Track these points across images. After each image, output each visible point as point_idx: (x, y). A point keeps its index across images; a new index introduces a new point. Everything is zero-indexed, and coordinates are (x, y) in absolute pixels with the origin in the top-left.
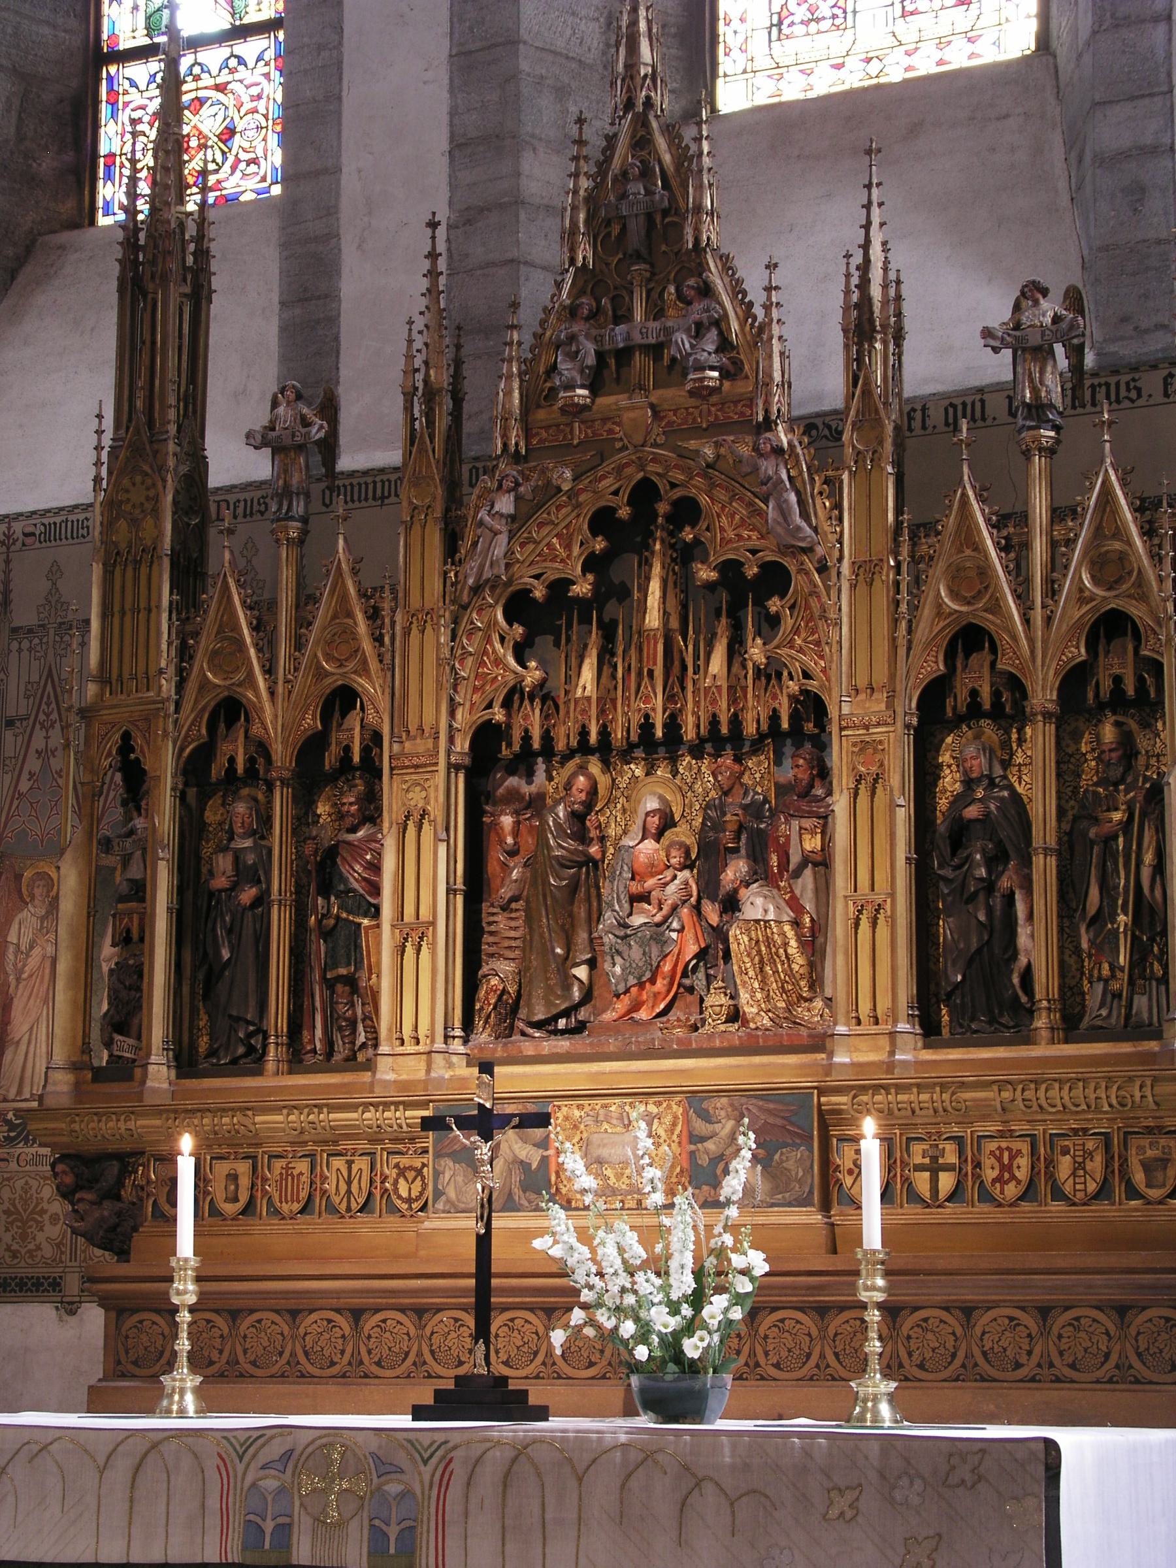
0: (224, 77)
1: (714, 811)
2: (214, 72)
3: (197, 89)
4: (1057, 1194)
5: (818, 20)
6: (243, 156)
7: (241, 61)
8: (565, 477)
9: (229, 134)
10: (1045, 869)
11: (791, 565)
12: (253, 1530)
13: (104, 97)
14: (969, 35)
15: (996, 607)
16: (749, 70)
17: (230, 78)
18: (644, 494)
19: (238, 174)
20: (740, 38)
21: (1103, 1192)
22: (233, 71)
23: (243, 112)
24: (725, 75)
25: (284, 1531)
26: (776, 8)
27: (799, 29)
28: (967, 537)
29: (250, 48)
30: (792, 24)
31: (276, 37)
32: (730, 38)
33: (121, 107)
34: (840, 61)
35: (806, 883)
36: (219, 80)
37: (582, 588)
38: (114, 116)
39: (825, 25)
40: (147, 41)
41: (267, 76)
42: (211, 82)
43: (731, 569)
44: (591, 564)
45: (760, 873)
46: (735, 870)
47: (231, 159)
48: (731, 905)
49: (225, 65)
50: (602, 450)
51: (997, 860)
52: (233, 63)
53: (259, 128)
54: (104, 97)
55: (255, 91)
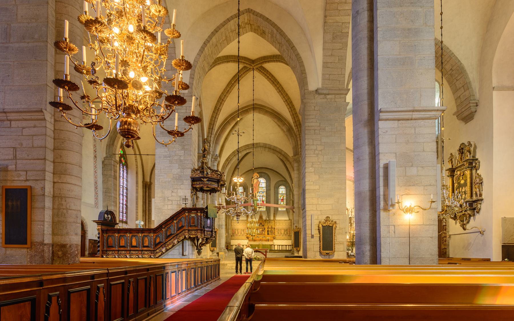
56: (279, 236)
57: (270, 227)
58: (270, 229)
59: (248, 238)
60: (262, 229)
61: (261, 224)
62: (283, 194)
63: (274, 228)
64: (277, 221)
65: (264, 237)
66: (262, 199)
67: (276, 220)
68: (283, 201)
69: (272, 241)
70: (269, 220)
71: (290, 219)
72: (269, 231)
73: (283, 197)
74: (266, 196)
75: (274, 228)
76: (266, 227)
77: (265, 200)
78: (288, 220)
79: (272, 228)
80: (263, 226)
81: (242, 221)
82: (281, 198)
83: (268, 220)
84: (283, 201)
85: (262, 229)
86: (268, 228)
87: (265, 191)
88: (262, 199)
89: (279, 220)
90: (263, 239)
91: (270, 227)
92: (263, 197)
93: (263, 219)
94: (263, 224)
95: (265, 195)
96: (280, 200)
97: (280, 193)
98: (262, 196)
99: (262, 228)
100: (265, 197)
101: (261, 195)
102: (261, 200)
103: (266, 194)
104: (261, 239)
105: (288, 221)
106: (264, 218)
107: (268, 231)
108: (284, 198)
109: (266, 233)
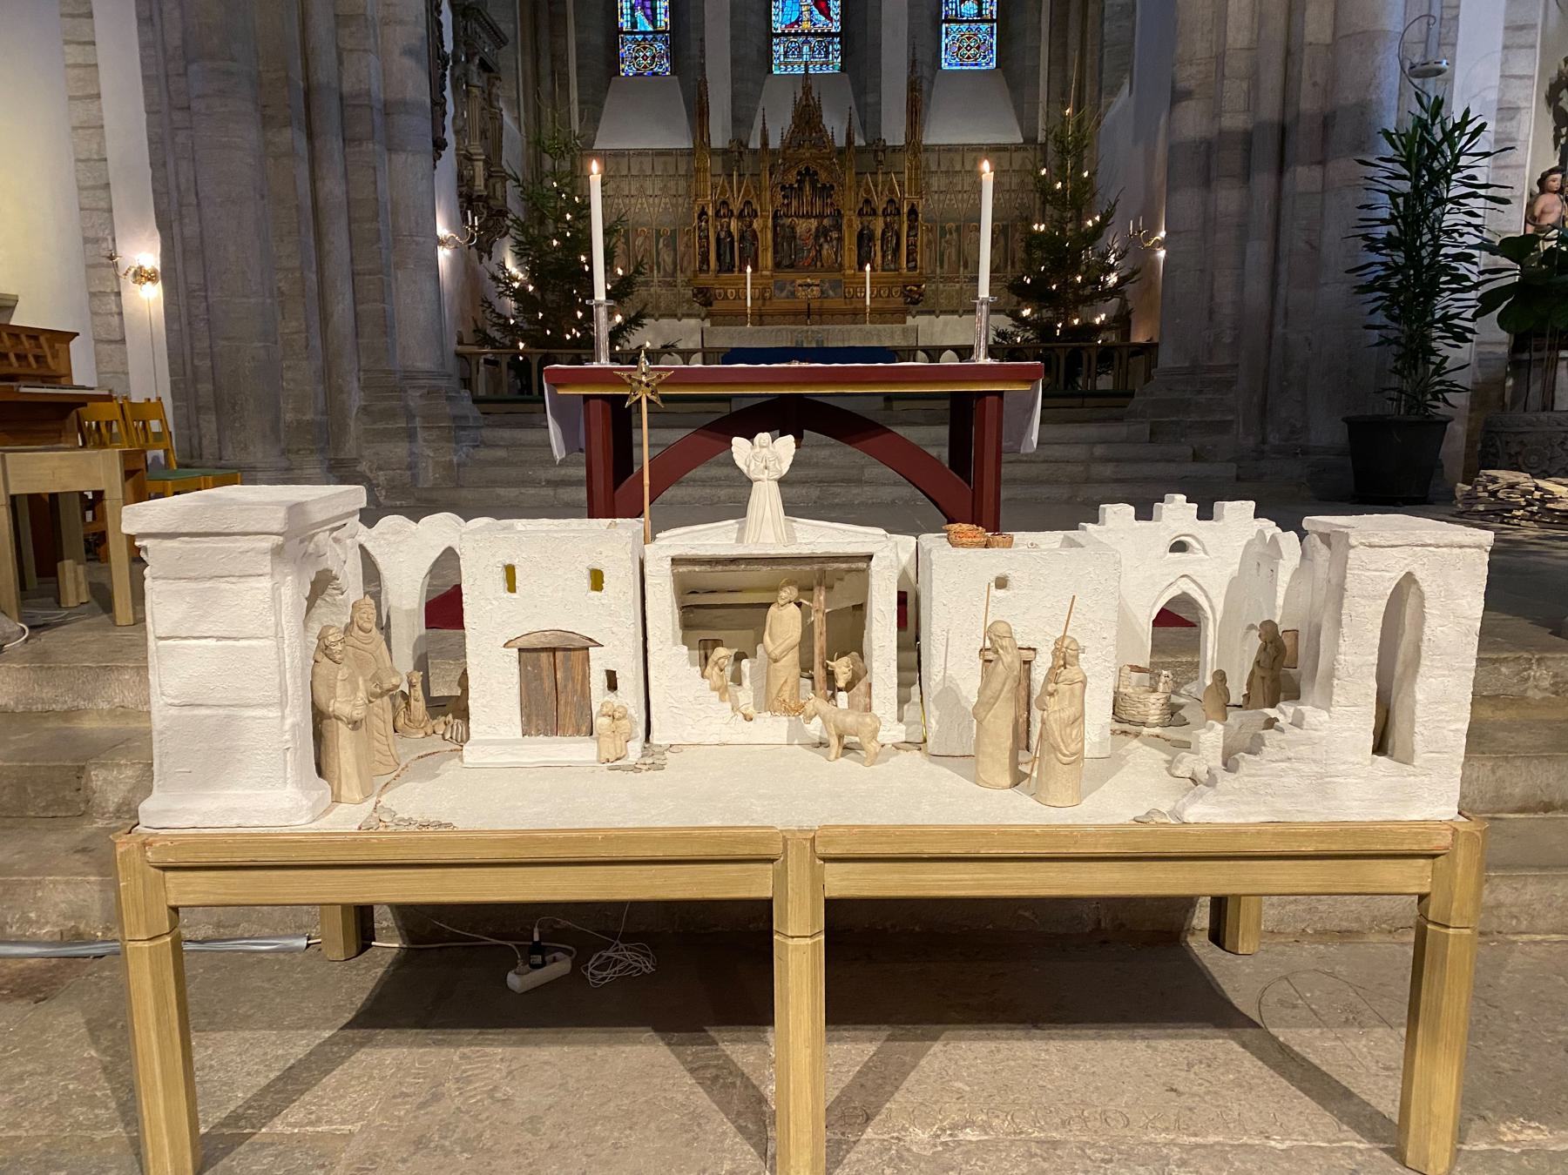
1: (817, 229)
4: (881, 296)
8: (793, 164)
9: (654, 57)
10: (879, 243)
11: (835, 185)
12: (797, 342)
15: (872, 196)
18: (807, 169)
21: (888, 296)
25: (802, 342)
28: (867, 184)
35: (835, 243)
37: (796, 186)
43: (824, 185)
44: (797, 181)
45: (826, 241)
46: (822, 240)
48: (821, 246)
50: (801, 160)
51: (870, 240)
56: (946, 280)
57: (880, 204)
58: (879, 225)
59: (705, 297)
60: (814, 223)
61: (808, 174)
63: (913, 212)
64: (933, 158)
65: (836, 285)
67: (927, 149)
69: (899, 315)
70: (877, 150)
71: (1030, 140)
72: (871, 238)
75: (913, 212)
76: (849, 202)
78: (1017, 148)
79: (893, 208)
80: (826, 191)
81: (659, 161)
83: (860, 150)
85: (814, 223)
86: (866, 209)
89: (950, 149)
90: (828, 304)
91: (880, 204)
93: (821, 130)
94: (823, 176)
99: (817, 211)
104: (815, 305)
105: (1018, 157)
106: (835, 126)
107: (860, 235)
109: (850, 256)
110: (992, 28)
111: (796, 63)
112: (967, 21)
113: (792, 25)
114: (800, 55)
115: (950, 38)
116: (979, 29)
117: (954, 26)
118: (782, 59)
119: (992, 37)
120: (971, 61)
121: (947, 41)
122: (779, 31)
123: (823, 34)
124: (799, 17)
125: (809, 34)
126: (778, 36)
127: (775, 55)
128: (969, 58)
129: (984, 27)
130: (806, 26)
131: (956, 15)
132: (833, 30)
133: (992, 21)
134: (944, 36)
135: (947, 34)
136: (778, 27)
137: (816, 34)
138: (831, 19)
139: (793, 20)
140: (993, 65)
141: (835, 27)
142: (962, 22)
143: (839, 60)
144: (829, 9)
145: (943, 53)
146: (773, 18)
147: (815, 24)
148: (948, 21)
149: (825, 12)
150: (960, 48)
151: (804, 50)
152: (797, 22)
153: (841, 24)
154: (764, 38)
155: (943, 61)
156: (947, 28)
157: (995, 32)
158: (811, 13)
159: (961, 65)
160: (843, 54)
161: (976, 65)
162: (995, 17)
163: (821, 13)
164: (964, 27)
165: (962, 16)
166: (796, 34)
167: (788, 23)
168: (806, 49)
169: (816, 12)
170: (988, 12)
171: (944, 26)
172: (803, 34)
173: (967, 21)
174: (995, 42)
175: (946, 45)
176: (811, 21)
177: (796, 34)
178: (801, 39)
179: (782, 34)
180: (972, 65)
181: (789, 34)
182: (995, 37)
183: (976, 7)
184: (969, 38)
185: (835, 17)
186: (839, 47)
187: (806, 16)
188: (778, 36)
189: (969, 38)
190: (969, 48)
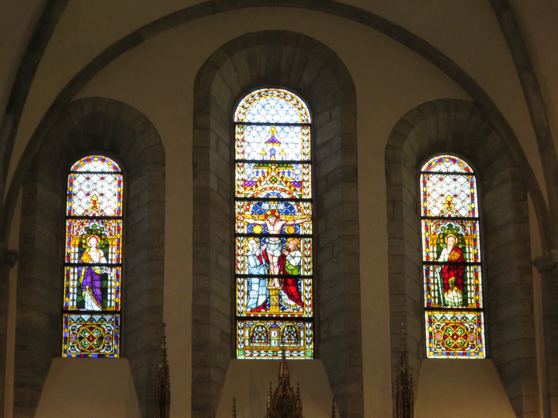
0: (100, 323)
2: (97, 320)
3: (91, 325)
5: (261, 340)
6: (106, 345)
7: (105, 320)
13: (64, 322)
14: (298, 350)
16: (244, 348)
17: (101, 323)
19: (104, 350)
20: (242, 340)
22: (102, 322)
23: (105, 333)
24: (238, 349)
26: (251, 335)
27: (257, 341)
29: (108, 317)
30: (255, 339)
31: (116, 316)
32: (239, 340)
33: (69, 325)
34: (267, 350)
36: (98, 323)
38: (67, 327)
39: (263, 341)
40: (77, 309)
41: (113, 325)
42: (95, 323)
47: (102, 345)
49: (100, 320)
52: (102, 320)
53: (110, 338)
54: (64, 322)
55: (109, 328)
62: (460, 219)
66: (282, 260)
68: (461, 285)
73: (459, 249)
74: (315, 237)
77: (307, 270)
82: (445, 256)
84: (461, 285)
87: (308, 193)
88: (282, 260)
92: (291, 243)
95: (307, 228)
96: (435, 274)
97: (435, 212)
98: (282, 236)
100: (307, 245)
101: (274, 229)
102: (276, 271)
103: (315, 219)
108: (470, 257)
110: (479, 318)
111: (263, 348)
112: (452, 309)
113: (258, 309)
114: (268, 339)
115: (434, 326)
116: (465, 319)
117: (438, 315)
118: (247, 343)
119: (479, 325)
120: (458, 351)
121: (431, 329)
122: (244, 315)
123: (292, 319)
124: (266, 301)
125: (278, 318)
126: (243, 319)
127: (240, 340)
128: (456, 347)
129: (471, 316)
130: (274, 311)
131: (440, 303)
132: (305, 315)
133: (478, 310)
134: (427, 324)
135: (431, 322)
136: (242, 309)
137: (285, 319)
138: (303, 305)
139: (260, 303)
140: (482, 355)
141: (308, 312)
142: (447, 310)
143: (312, 346)
144: (300, 294)
145: (427, 341)
146: (238, 301)
147: (284, 309)
148: (430, 309)
149: (296, 297)
150: (445, 337)
151: (273, 335)
152: (265, 306)
153: (313, 310)
154: (227, 322)
155: (428, 350)
156: (430, 317)
157: (483, 321)
158: (280, 297)
159: (448, 354)
160: (316, 340)
161: (464, 354)
162: (481, 306)
163: (291, 297)
164: (449, 315)
165: (445, 305)
166: (263, 319)
167: (254, 306)
168: (274, 334)
169: (285, 297)
170: (473, 301)
171: (427, 314)
172: (270, 318)
173: (452, 309)
174: (483, 332)
175: (431, 334)
176: (280, 305)
177: (263, 319)
178: (269, 324)
179: (248, 318)
180: (459, 354)
181: (256, 318)
182: (483, 326)
183: (460, 296)
184: (455, 327)
185: (306, 302)
186: (311, 332)
187: (274, 300)
188: (243, 319)
189: (455, 327)
190: (455, 337)
